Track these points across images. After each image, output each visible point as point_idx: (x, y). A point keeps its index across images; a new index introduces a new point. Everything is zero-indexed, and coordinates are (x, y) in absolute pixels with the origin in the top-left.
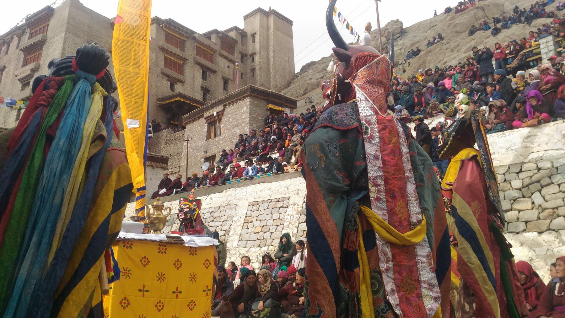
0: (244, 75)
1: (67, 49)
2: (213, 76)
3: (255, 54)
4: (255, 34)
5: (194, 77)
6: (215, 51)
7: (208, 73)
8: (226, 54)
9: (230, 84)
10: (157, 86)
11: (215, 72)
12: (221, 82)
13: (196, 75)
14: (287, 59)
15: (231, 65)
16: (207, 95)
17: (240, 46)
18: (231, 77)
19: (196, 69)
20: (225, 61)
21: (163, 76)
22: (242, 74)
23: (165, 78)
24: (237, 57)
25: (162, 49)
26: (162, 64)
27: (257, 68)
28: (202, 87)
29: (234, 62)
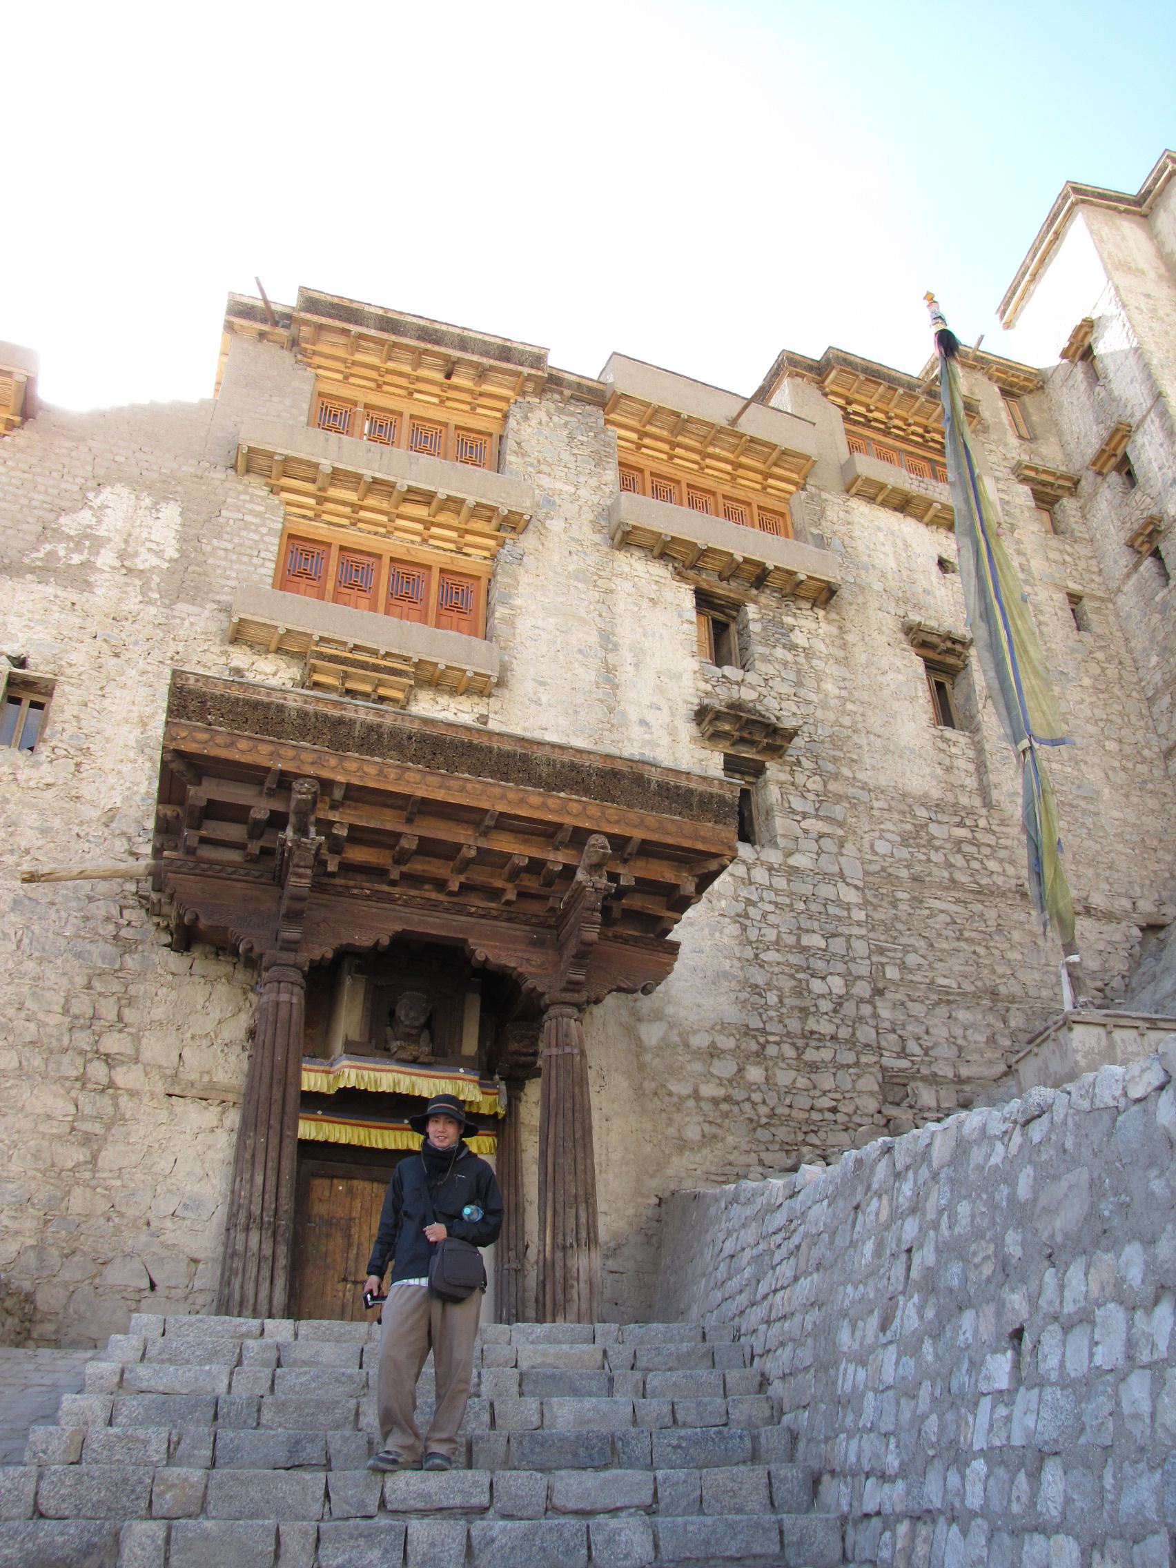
0: (1088, 605)
2: (808, 627)
3: (1121, 434)
4: (1088, 327)
5: (608, 641)
6: (800, 466)
7: (751, 611)
8: (898, 477)
11: (824, 595)
12: (906, 673)
13: (626, 634)
16: (774, 771)
17: (1013, 441)
20: (908, 527)
22: (1075, 599)
28: (702, 714)
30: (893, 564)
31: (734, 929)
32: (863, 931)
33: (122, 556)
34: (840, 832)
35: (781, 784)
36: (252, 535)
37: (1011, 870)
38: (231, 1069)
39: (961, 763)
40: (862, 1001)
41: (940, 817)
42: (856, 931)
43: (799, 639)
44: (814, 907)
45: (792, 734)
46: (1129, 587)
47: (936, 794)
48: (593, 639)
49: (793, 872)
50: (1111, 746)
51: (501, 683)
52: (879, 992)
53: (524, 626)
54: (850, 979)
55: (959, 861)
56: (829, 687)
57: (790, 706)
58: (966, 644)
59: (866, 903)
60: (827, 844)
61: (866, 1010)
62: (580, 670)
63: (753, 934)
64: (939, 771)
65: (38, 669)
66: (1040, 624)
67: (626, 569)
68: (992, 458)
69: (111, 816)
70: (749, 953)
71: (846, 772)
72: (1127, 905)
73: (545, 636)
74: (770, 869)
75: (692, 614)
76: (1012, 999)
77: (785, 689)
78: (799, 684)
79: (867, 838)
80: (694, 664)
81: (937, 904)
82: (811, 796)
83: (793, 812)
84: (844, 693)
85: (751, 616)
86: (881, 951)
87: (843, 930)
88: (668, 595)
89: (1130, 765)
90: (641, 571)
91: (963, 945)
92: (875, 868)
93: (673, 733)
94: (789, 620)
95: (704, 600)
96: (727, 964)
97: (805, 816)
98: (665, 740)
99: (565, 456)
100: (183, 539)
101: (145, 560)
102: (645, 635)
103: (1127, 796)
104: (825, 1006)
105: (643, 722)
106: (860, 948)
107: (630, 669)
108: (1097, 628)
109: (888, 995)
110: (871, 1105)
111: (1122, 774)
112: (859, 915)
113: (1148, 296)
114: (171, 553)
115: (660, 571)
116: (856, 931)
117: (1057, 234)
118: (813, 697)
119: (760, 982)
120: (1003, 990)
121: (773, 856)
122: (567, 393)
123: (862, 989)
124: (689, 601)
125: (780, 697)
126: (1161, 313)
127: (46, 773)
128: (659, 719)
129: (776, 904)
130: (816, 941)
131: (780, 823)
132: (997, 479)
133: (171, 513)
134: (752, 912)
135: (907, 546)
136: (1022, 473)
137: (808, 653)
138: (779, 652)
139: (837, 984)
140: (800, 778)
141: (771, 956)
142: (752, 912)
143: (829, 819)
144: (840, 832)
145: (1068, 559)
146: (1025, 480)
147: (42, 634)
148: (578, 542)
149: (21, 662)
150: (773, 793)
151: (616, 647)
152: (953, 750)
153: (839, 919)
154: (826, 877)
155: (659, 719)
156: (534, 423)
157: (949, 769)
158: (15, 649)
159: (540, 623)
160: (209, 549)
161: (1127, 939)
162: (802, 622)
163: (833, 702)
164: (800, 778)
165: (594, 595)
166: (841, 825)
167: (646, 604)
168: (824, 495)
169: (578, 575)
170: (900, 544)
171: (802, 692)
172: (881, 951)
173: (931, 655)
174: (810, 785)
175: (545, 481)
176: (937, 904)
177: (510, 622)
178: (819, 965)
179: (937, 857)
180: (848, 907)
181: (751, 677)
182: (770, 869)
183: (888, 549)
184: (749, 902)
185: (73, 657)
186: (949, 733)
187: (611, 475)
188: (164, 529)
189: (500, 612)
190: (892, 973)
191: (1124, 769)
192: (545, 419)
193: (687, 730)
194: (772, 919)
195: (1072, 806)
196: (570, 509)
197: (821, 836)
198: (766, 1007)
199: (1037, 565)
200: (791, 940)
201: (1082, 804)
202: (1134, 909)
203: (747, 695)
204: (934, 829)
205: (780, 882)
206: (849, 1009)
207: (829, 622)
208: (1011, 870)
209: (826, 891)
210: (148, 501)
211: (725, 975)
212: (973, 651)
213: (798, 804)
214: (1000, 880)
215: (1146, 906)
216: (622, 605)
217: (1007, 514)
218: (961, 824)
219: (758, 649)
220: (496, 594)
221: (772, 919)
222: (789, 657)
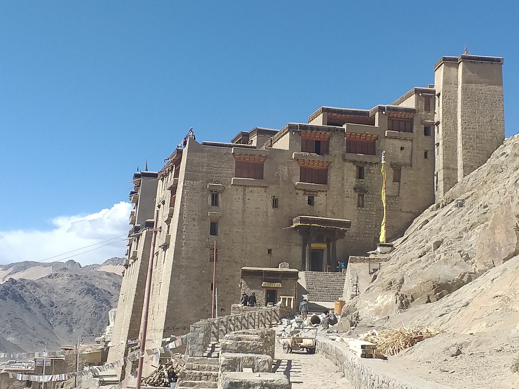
7: (365, 167)
14: (488, 119)
15: (407, 145)
16: (365, 195)
19: (345, 169)
23: (301, 193)
28: (355, 189)
38: (300, 242)
43: (372, 171)
54: (372, 225)
69: (287, 215)
74: (363, 211)
90: (348, 164)
93: (351, 191)
98: (349, 193)
101: (285, 179)
104: (368, 229)
110: (373, 241)
115: (351, 164)
121: (363, 209)
124: (355, 169)
149: (274, 197)
173: (395, 169)
178: (368, 224)
182: (363, 211)
185: (280, 195)
187: (345, 147)
193: (353, 191)
203: (363, 183)
206: (371, 229)
219: (365, 175)
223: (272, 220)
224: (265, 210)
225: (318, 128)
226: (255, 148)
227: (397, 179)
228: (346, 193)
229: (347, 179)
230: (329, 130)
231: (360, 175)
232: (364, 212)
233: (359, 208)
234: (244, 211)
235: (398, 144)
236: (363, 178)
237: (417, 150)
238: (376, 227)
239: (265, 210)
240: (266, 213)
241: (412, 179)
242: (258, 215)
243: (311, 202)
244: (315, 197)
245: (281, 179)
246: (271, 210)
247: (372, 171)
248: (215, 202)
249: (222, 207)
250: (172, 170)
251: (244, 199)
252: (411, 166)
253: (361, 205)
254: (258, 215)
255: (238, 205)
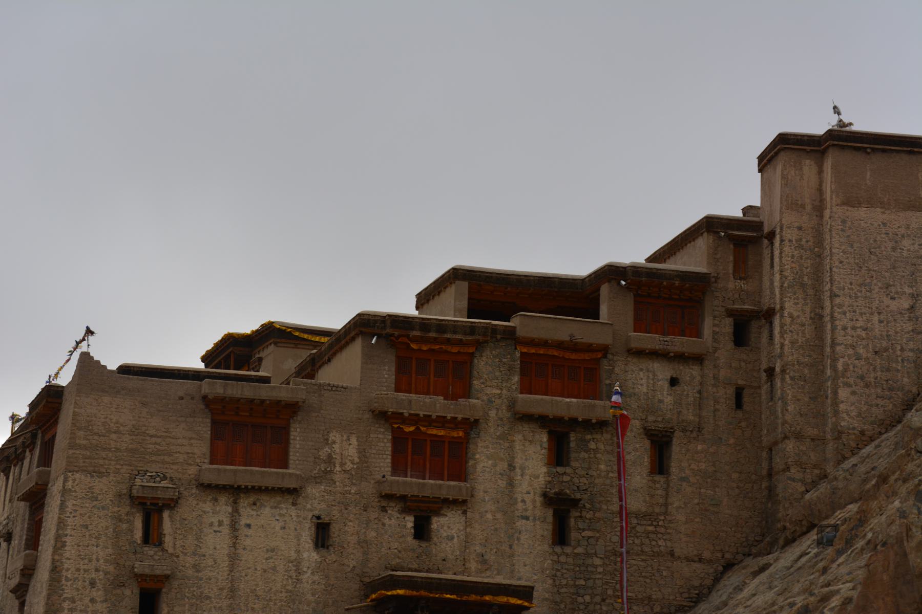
0: (746, 392)
1: (70, 521)
5: (511, 467)
7: (572, 436)
9: (677, 449)
10: (364, 543)
13: (518, 461)
14: (906, 304)
15: (689, 373)
16: (574, 513)
18: (690, 416)
21: (384, 504)
24: (714, 328)
25: (382, 416)
26: (383, 463)
27: (778, 369)
28: (544, 495)
29: (698, 359)
30: (645, 390)
31: (550, 582)
32: (600, 576)
33: (342, 464)
34: (598, 535)
35: (576, 518)
36: (382, 445)
37: (669, 544)
39: (659, 492)
40: (596, 603)
41: (642, 522)
42: (598, 576)
43: (592, 445)
44: (582, 568)
45: (580, 500)
46: (765, 387)
47: (644, 509)
48: (506, 465)
49: (578, 554)
50: (735, 476)
51: (472, 496)
52: (604, 600)
53: (479, 468)
54: (593, 596)
55: (647, 541)
56: (602, 467)
57: (584, 480)
58: (672, 433)
59: (604, 563)
60: (592, 541)
61: (598, 607)
62: (500, 482)
63: (557, 583)
64: (648, 499)
65: (325, 519)
66: (716, 410)
67: (520, 428)
68: (716, 302)
70: (556, 590)
71: (605, 507)
72: (719, 555)
73: (488, 470)
74: (567, 555)
75: (546, 445)
76: (657, 600)
77: (583, 472)
78: (589, 468)
79: (609, 536)
80: (544, 469)
81: (634, 562)
82: (587, 521)
83: (580, 529)
84: (609, 468)
85: (572, 439)
86: (607, 583)
87: (593, 576)
88: (537, 436)
89: (742, 485)
90: (526, 428)
91: (641, 579)
92: (609, 548)
93: (534, 501)
94: (589, 437)
95: (550, 433)
96: (547, 596)
97: (584, 530)
98: (530, 506)
99: (497, 374)
100: (359, 452)
101: (349, 466)
102: (526, 460)
103: (735, 502)
105: (523, 501)
106: (599, 582)
107: (519, 478)
108: (746, 407)
109: (607, 601)
111: (737, 491)
112: (600, 570)
113: (800, 228)
114: (357, 460)
116: (598, 576)
117: (776, 154)
118: (595, 474)
119: (558, 600)
120: (654, 597)
121: (568, 550)
122: (499, 337)
123: (598, 599)
125: (581, 476)
126: (803, 242)
127: (333, 557)
128: (528, 498)
129: (567, 570)
130: (582, 582)
131: (574, 535)
132: (715, 317)
133: (354, 440)
134: (559, 574)
135: (654, 375)
136: (730, 313)
137: (596, 451)
138: (583, 455)
139: (587, 598)
140: (584, 513)
141: (563, 590)
142: (559, 574)
143: (593, 530)
144: (598, 535)
145: (743, 364)
146: (729, 317)
147: (323, 506)
148: (501, 419)
149: (318, 518)
150: (572, 521)
151: (515, 468)
152: (657, 486)
153: (592, 572)
154: (588, 555)
155: (528, 498)
156: (484, 358)
157: (652, 496)
158: (317, 513)
159: (485, 464)
160: (368, 454)
161: (716, 571)
162: (596, 436)
163: (603, 474)
164: (584, 513)
165: (507, 445)
166: (598, 531)
167: (527, 444)
168: (615, 358)
169: (499, 438)
170: (651, 376)
171: (591, 472)
172: (607, 583)
174: (588, 516)
175: (488, 391)
176: (634, 562)
177: (474, 466)
178: (582, 591)
179: (637, 541)
180: (596, 567)
181: (568, 470)
182: (567, 555)
183: (644, 381)
184: (558, 570)
185: (335, 512)
186: (657, 478)
187: (516, 378)
188: (352, 452)
189: (471, 463)
190: (610, 592)
191: (738, 487)
192: (489, 353)
193: (539, 500)
194: (565, 576)
195: (706, 510)
196: (498, 401)
197: (589, 538)
198: (560, 609)
199: (723, 373)
200: (572, 583)
201: (712, 509)
202: (723, 557)
204: (639, 528)
205: (570, 560)
206: (591, 607)
207: (607, 432)
208: (669, 544)
209: (589, 561)
210: (345, 437)
211: (546, 599)
212: (678, 434)
213: (581, 526)
214: (662, 548)
215: (727, 556)
216: (518, 446)
217: (715, 340)
218: (651, 525)
219: (573, 455)
220: (469, 455)
221: (565, 576)
222: (586, 456)
223: (314, 582)
224: (293, 555)
225: (441, 327)
226: (266, 380)
227: (660, 465)
228: (520, 506)
229: (523, 468)
230: (472, 329)
231: (558, 455)
232: (570, 560)
233: (558, 549)
234: (234, 558)
235: (663, 371)
236: (568, 465)
237: (714, 385)
238: (604, 600)
239: (293, 555)
240: (297, 563)
241: (703, 466)
242: (274, 569)
243: (422, 532)
244: (435, 519)
245: (338, 468)
246: (311, 556)
247: (592, 445)
248: (151, 535)
249: (171, 550)
250: (33, 444)
251: (234, 527)
252: (700, 430)
253: (560, 536)
254: (274, 569)
255: (216, 543)
